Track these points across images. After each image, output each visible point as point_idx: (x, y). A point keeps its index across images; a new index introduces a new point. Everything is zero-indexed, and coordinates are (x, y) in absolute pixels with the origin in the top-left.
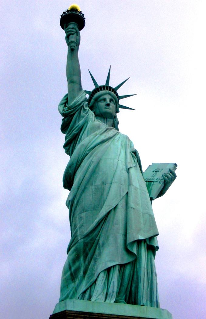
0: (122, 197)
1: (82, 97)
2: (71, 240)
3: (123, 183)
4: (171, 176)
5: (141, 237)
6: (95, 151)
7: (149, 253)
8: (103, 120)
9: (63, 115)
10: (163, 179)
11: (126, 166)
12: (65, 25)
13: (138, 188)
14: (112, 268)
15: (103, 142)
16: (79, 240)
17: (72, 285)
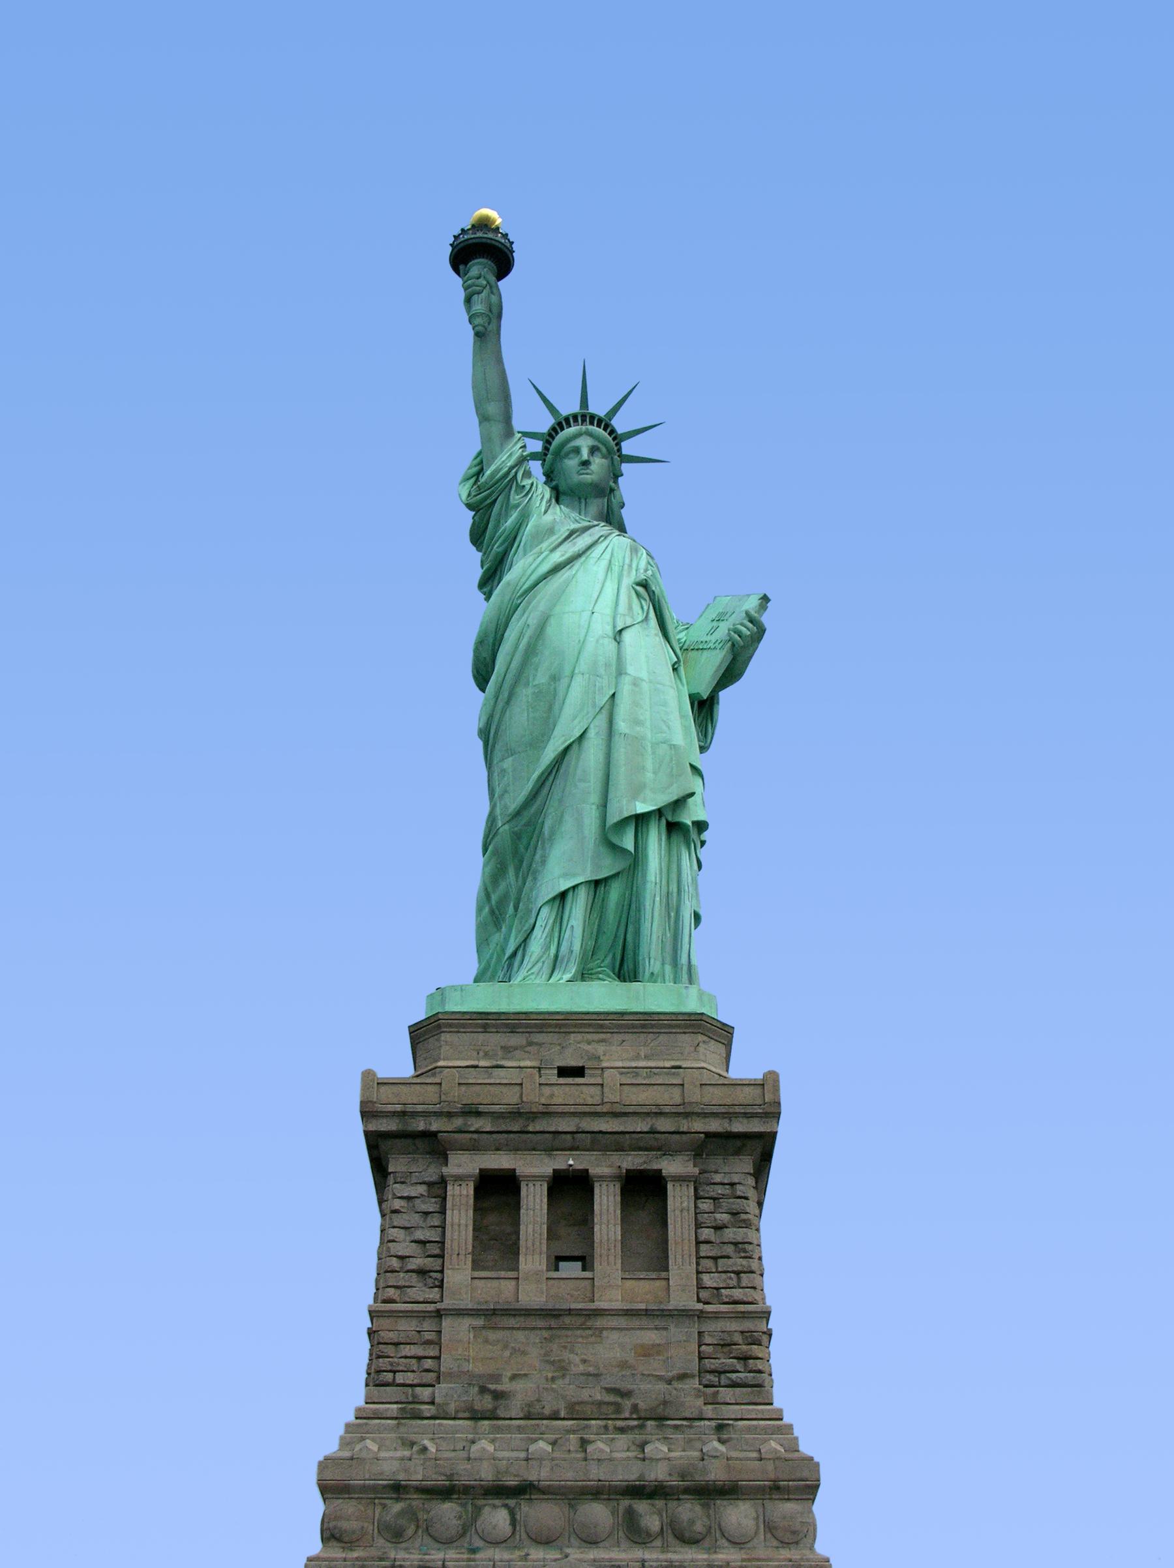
0: (598, 709)
1: (511, 455)
2: (485, 831)
3: (602, 671)
4: (748, 629)
5: (641, 808)
6: (535, 597)
7: (675, 841)
8: (576, 503)
9: (470, 506)
10: (729, 640)
11: (614, 627)
12: (461, 267)
13: (643, 680)
14: (570, 894)
15: (557, 569)
16: (499, 828)
17: (497, 938)
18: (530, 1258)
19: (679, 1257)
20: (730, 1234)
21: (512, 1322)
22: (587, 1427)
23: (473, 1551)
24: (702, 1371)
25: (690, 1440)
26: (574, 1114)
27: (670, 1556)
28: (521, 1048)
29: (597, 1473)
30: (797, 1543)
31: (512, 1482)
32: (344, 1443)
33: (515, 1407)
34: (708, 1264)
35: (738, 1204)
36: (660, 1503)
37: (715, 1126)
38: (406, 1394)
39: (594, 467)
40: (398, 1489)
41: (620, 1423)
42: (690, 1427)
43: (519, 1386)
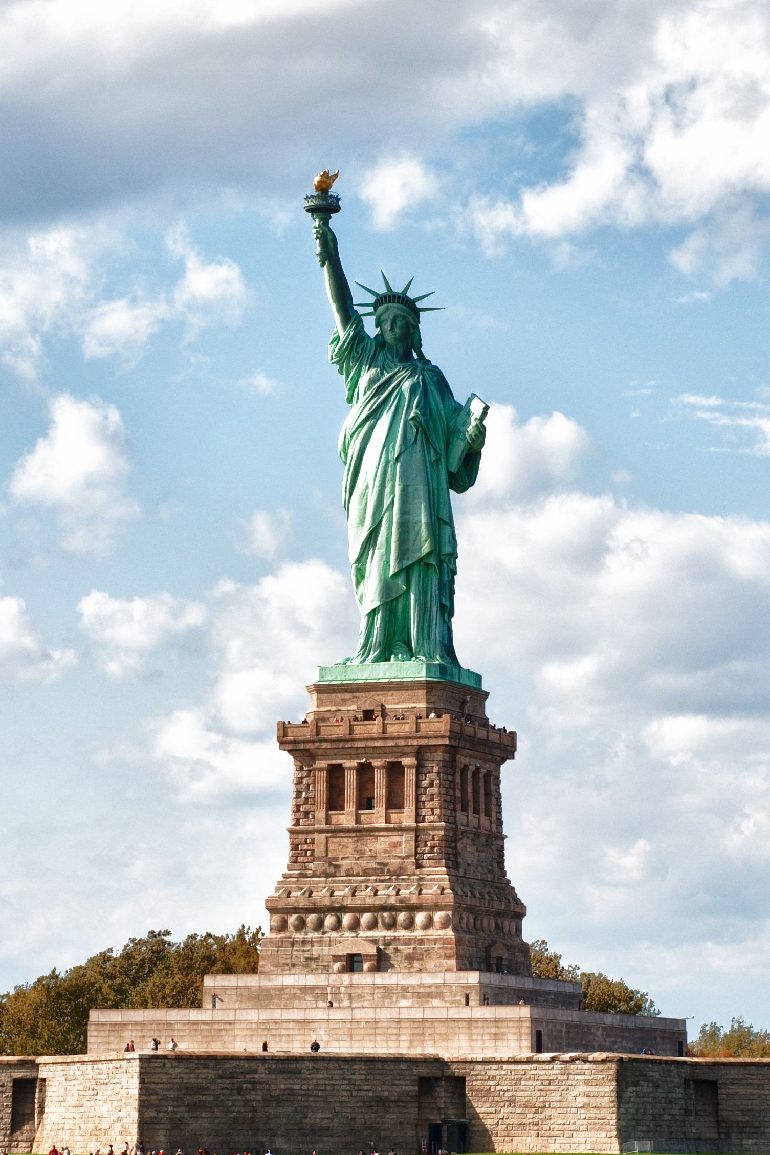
1: (349, 334)
5: (407, 563)
14: (377, 610)
21: (343, 835)
23: (324, 933)
24: (416, 853)
25: (408, 885)
27: (397, 934)
28: (350, 699)
29: (369, 901)
31: (337, 905)
32: (277, 890)
37: (423, 742)
38: (302, 867)
39: (397, 330)
40: (295, 910)
41: (382, 878)
43: (344, 862)
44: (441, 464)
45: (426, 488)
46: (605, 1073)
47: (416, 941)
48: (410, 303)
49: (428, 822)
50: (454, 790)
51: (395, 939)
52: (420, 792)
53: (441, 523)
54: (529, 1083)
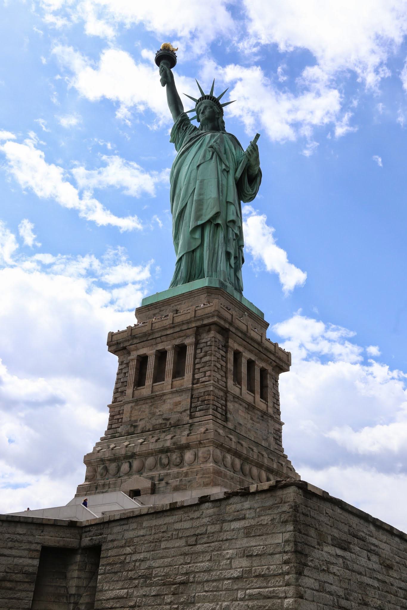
5: (200, 223)
13: (204, 180)
18: (148, 380)
19: (188, 370)
20: (204, 360)
22: (155, 432)
23: (119, 477)
26: (160, 331)
28: (158, 313)
29: (152, 446)
30: (206, 461)
33: (139, 430)
34: (197, 370)
35: (207, 349)
36: (169, 454)
37: (199, 323)
40: (102, 461)
42: (183, 427)
44: (230, 174)
45: (216, 180)
46: (276, 512)
47: (182, 474)
48: (215, 100)
49: (201, 383)
50: (226, 362)
51: (167, 475)
52: (197, 361)
53: (228, 205)
54: (169, 545)
